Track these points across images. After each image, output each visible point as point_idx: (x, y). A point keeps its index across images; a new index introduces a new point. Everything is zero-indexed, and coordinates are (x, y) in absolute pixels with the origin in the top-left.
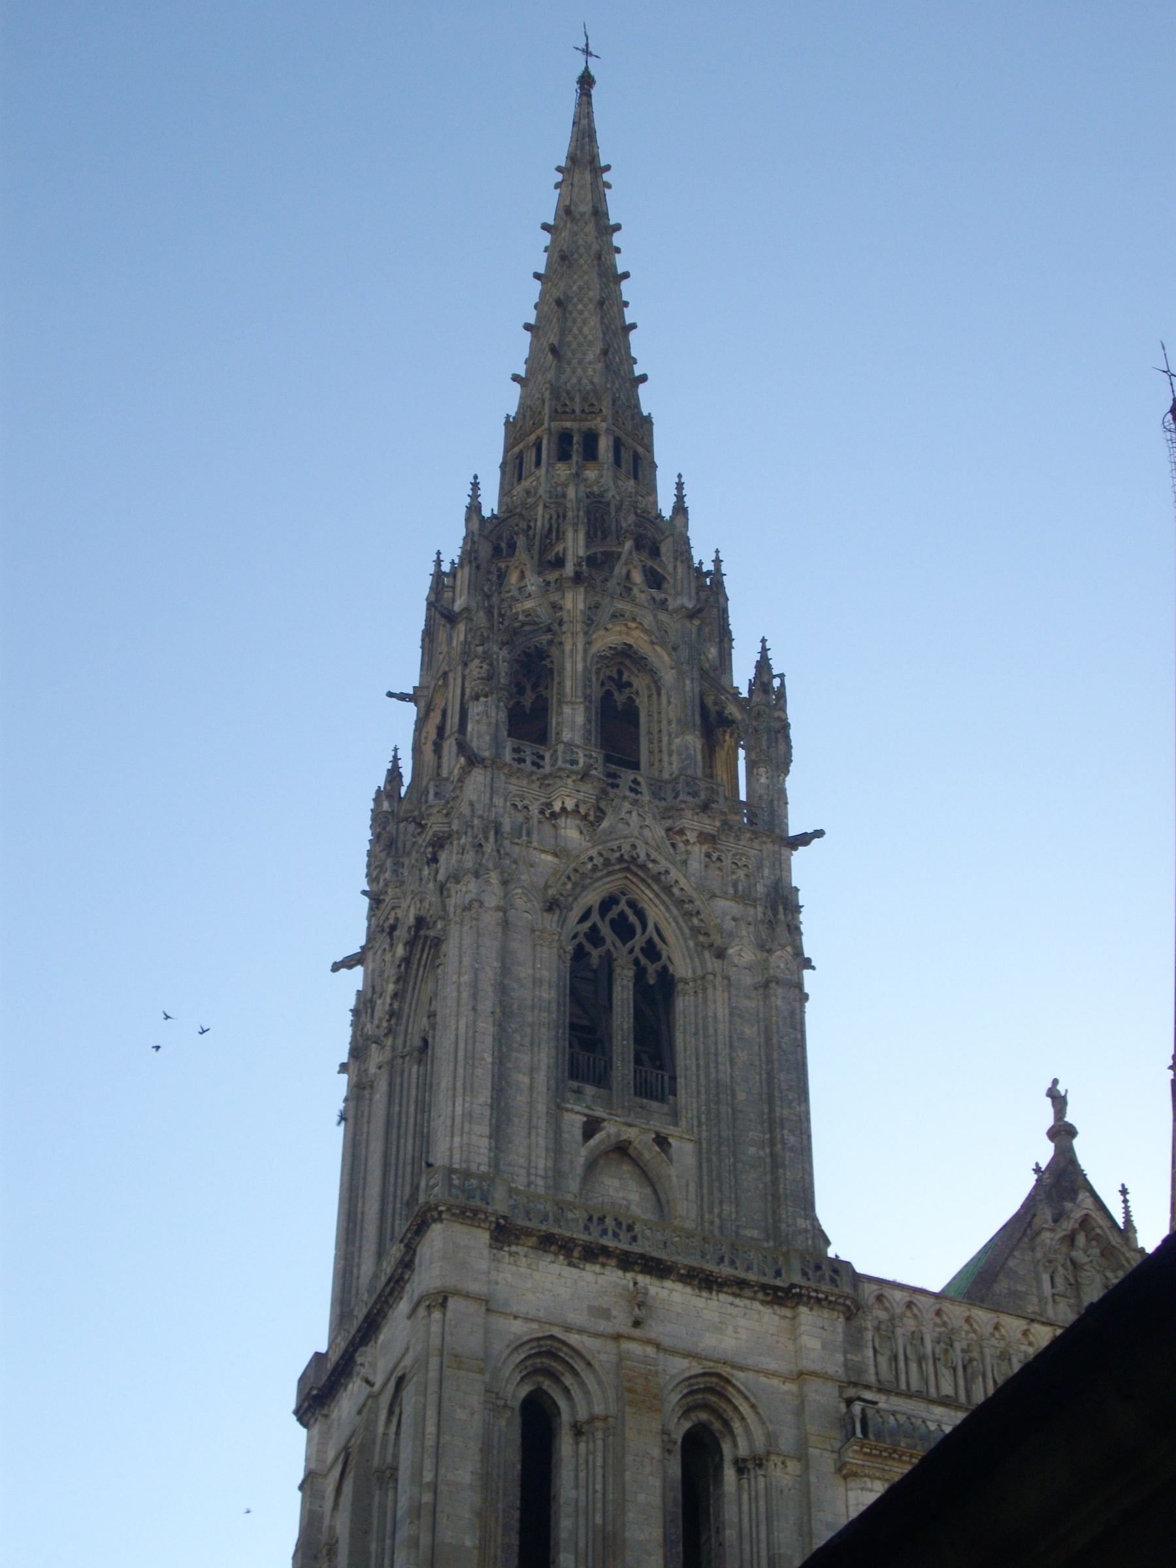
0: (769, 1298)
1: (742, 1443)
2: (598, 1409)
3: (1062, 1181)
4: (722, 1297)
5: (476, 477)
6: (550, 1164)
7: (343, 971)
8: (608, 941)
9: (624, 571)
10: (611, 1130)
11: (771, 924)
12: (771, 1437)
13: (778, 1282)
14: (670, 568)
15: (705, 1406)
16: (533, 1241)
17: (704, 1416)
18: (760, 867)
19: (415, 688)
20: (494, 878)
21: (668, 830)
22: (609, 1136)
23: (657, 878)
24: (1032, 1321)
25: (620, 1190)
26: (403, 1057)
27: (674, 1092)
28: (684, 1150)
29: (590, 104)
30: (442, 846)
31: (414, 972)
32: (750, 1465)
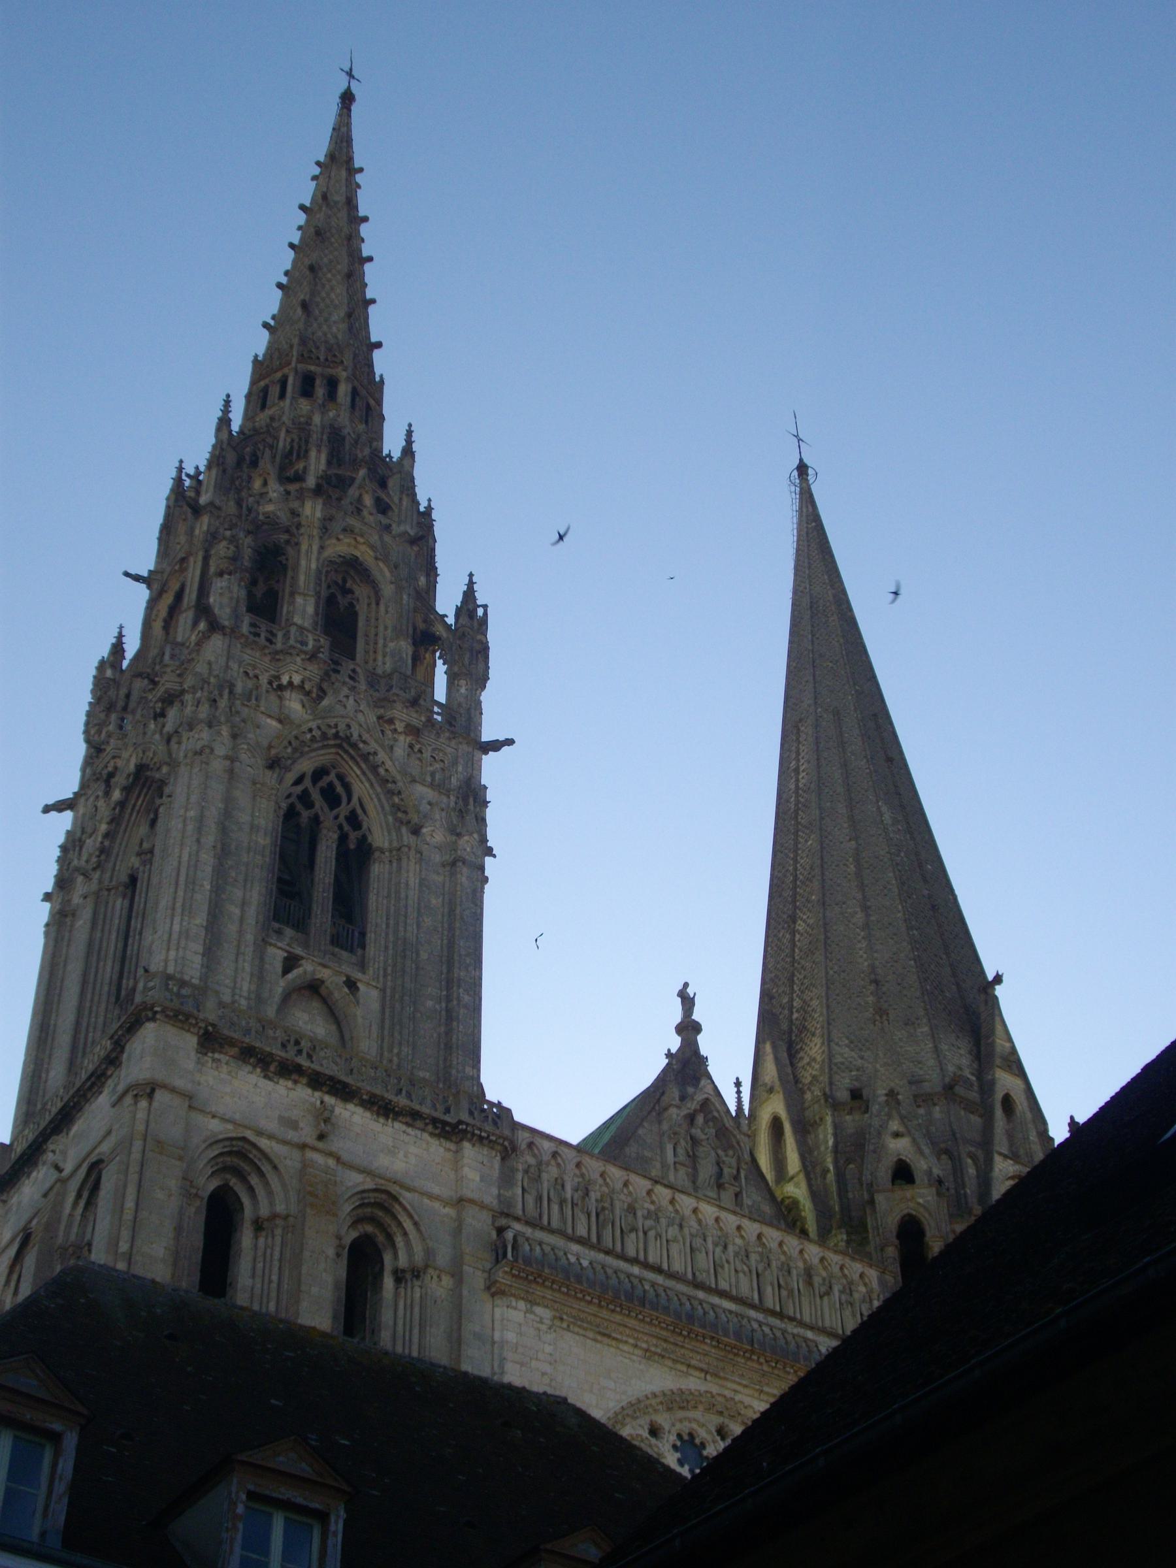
0: (437, 1132)
1: (402, 1254)
2: (280, 1208)
3: (687, 1066)
4: (397, 1125)
5: (228, 396)
6: (253, 987)
7: (53, 813)
8: (317, 805)
9: (357, 494)
10: (308, 968)
11: (462, 814)
12: (429, 1253)
13: (447, 1118)
14: (396, 499)
15: (372, 1220)
16: (234, 1051)
17: (369, 1228)
18: (455, 763)
19: (150, 571)
20: (225, 731)
21: (380, 718)
22: (305, 972)
23: (365, 757)
24: (656, 1182)
25: (309, 1021)
26: (109, 890)
27: (363, 947)
28: (370, 995)
29: (350, 116)
30: (171, 703)
31: (127, 816)
32: (408, 1276)
